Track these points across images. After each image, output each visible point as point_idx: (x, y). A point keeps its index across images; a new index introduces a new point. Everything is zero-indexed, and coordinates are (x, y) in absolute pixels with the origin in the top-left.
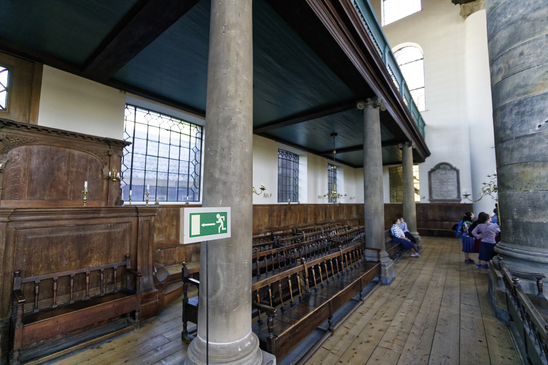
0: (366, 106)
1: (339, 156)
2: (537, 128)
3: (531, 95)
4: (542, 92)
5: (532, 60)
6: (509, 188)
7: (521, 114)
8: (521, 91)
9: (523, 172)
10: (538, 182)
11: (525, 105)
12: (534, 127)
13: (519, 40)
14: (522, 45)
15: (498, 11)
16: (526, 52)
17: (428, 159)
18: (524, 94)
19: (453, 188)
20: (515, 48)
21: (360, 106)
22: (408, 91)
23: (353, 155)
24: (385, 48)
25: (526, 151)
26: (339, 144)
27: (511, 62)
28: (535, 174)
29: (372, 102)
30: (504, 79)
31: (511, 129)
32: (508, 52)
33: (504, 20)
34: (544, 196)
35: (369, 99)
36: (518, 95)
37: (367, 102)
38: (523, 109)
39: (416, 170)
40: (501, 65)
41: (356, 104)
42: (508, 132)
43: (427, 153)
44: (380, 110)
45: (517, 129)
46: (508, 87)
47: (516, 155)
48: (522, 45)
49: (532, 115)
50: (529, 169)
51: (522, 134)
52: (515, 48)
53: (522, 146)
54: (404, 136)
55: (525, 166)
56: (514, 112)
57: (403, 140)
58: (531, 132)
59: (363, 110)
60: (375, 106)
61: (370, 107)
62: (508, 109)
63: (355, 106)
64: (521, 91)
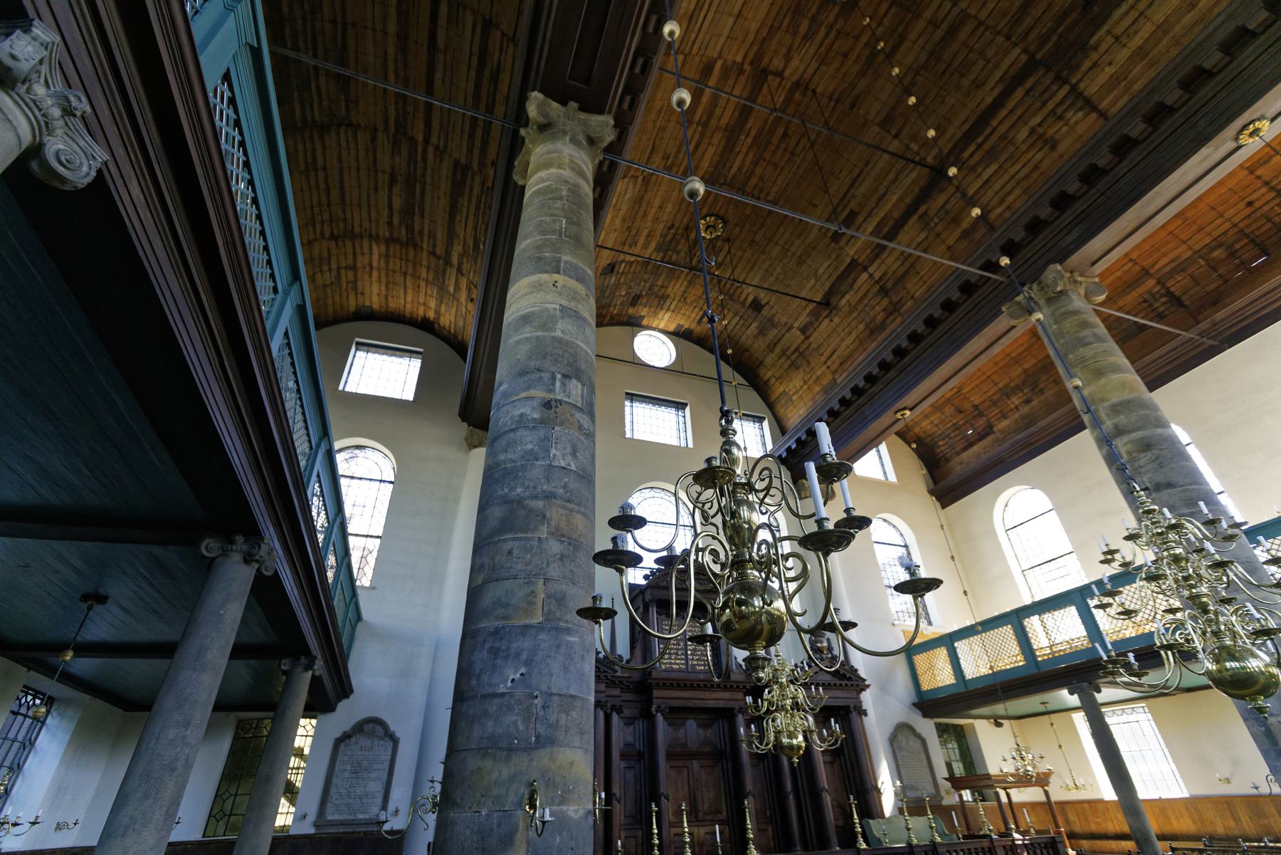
0: (225, 553)
1: (84, 666)
2: (509, 684)
3: (511, 622)
4: (522, 623)
5: (519, 567)
6: (454, 804)
7: (495, 652)
8: (500, 611)
9: (480, 769)
10: (496, 791)
11: (501, 639)
12: (506, 681)
13: (512, 530)
14: (514, 539)
15: (497, 475)
16: (515, 552)
17: (343, 706)
18: (505, 618)
19: (376, 787)
20: (505, 540)
21: (209, 547)
22: (344, 534)
23: (136, 670)
24: (321, 440)
25: (490, 724)
26: (101, 627)
27: (497, 558)
28: (495, 775)
29: (245, 548)
30: (485, 582)
31: (478, 677)
32: (496, 543)
33: (500, 493)
34: (499, 825)
35: (240, 539)
36: (497, 618)
37: (232, 542)
38: (498, 645)
39: (305, 733)
40: (486, 559)
41: (202, 539)
42: (474, 682)
43: (345, 689)
44: (258, 570)
45: (485, 678)
46: (487, 599)
47: (477, 732)
48: (514, 539)
49: (506, 658)
50: (487, 764)
51: (490, 690)
52: (505, 540)
53: (486, 714)
54: (301, 639)
55: (484, 756)
56: (487, 646)
57: (299, 651)
58: (502, 689)
59: (213, 560)
60: (248, 559)
61: (236, 558)
62: (480, 639)
63: (196, 543)
64: (500, 611)
